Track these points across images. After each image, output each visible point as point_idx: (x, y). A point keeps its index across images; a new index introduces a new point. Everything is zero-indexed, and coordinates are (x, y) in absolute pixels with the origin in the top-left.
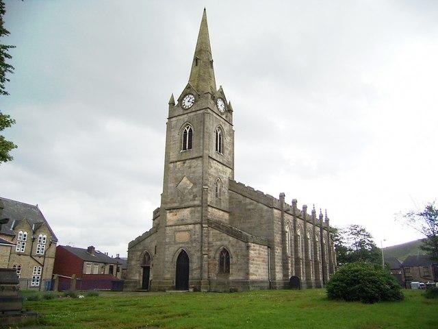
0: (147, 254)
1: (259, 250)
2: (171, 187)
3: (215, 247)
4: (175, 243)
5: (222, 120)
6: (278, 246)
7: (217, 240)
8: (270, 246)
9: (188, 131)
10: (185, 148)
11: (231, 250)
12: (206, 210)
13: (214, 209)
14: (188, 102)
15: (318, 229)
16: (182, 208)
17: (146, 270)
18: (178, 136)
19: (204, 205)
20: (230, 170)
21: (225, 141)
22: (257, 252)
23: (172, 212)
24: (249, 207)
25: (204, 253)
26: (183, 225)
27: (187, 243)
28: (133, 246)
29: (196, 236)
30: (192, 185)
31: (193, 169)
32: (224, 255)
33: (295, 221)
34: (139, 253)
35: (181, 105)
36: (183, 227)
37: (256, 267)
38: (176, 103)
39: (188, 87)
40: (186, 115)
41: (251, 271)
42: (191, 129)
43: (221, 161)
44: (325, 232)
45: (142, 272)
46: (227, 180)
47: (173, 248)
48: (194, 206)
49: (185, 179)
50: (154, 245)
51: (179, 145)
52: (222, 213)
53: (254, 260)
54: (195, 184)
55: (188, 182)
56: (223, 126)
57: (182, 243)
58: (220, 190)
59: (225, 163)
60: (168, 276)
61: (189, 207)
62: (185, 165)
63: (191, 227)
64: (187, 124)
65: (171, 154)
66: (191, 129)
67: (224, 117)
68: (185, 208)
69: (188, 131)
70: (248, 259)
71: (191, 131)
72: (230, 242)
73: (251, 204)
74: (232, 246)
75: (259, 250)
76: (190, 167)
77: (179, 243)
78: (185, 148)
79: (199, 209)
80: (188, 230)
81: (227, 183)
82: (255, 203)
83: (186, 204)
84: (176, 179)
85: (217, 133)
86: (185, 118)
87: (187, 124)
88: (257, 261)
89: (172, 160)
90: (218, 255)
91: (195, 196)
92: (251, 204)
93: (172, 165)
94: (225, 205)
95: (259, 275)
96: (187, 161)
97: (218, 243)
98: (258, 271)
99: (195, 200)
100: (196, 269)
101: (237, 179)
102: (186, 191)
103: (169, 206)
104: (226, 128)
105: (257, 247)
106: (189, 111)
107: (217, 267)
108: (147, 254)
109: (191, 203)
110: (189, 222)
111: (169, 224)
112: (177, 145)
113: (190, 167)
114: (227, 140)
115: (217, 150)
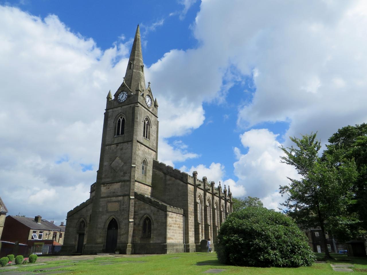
1: (175, 218)
2: (106, 166)
3: (141, 216)
4: (107, 212)
5: (149, 112)
6: (192, 215)
7: (141, 210)
8: (185, 215)
10: (118, 134)
11: (153, 217)
12: (134, 184)
15: (223, 201)
16: (114, 183)
17: (81, 235)
19: (132, 180)
20: (155, 153)
21: (151, 129)
22: (174, 219)
23: (106, 186)
24: (168, 182)
25: (131, 220)
26: (113, 196)
28: (71, 215)
29: (125, 206)
30: (123, 164)
32: (147, 222)
33: (205, 195)
34: (76, 221)
36: (114, 199)
37: (173, 232)
38: (113, 98)
39: (123, 85)
40: (120, 108)
42: (124, 118)
43: (148, 145)
44: (228, 204)
45: (77, 238)
46: (152, 160)
47: (105, 216)
48: (124, 181)
49: (118, 158)
50: (90, 212)
52: (146, 187)
53: (171, 226)
55: (120, 161)
56: (150, 117)
57: (112, 212)
58: (146, 168)
59: (150, 147)
60: (100, 240)
61: (119, 182)
62: (118, 147)
63: (120, 198)
65: (107, 138)
66: (124, 118)
67: (150, 110)
68: (117, 182)
70: (166, 226)
71: (123, 120)
72: (152, 211)
73: (170, 180)
74: (154, 214)
75: (175, 218)
76: (122, 149)
78: (118, 134)
80: (118, 201)
81: (152, 163)
82: (174, 179)
85: (145, 123)
88: (173, 227)
90: (142, 222)
92: (170, 180)
93: (107, 148)
94: (149, 181)
96: (119, 145)
97: (142, 212)
98: (174, 236)
101: (160, 160)
102: (118, 168)
103: (103, 181)
104: (152, 119)
105: (174, 215)
107: (141, 232)
108: (83, 222)
109: (123, 178)
110: (119, 194)
111: (102, 196)
113: (122, 149)
114: (153, 128)
115: (144, 136)
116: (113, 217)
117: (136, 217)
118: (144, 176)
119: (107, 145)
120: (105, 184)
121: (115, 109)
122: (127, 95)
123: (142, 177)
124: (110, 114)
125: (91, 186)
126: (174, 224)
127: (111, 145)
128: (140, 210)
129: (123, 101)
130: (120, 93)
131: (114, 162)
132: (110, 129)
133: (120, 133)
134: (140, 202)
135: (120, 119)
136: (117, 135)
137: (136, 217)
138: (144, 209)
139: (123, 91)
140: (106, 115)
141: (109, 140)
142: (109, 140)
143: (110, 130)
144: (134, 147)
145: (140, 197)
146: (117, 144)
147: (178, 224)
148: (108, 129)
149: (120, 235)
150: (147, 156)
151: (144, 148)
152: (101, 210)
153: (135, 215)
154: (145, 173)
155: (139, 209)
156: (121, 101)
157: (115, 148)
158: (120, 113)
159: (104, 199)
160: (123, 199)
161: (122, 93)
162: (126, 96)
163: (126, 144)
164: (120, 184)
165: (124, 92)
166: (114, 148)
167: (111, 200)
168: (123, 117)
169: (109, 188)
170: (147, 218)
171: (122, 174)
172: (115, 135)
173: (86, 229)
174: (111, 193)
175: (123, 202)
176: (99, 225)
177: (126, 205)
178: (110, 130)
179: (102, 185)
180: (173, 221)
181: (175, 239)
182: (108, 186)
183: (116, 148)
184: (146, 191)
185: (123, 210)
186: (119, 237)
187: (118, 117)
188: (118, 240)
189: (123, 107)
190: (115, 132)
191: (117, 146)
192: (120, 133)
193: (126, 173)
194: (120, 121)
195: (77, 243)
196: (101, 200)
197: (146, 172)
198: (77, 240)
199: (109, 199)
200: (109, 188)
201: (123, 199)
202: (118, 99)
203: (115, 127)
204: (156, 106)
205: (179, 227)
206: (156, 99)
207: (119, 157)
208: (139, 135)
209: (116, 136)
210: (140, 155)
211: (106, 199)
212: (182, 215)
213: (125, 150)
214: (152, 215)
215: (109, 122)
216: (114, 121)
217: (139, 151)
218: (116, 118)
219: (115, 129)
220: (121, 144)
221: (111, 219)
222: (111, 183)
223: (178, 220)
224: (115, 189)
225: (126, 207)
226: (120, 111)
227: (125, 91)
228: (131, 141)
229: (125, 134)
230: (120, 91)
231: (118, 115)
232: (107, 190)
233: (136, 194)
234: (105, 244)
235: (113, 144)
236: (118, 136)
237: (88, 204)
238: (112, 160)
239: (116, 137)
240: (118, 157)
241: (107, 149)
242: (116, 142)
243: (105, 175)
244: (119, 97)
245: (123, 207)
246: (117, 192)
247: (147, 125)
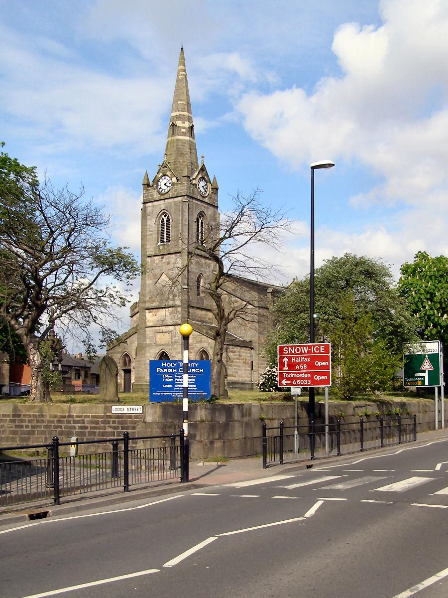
0: (127, 355)
1: (239, 352)
2: (149, 285)
3: (196, 349)
4: (157, 345)
9: (165, 221)
16: (162, 308)
18: (153, 224)
27: (168, 345)
29: (177, 338)
34: (119, 355)
35: (157, 187)
40: (162, 201)
41: (229, 372)
45: (123, 375)
49: (164, 276)
50: (135, 345)
51: (155, 236)
53: (232, 362)
57: (163, 345)
61: (169, 307)
62: (164, 260)
65: (148, 246)
67: (206, 200)
69: (165, 221)
71: (168, 220)
73: (236, 302)
75: (239, 352)
76: (168, 263)
77: (160, 345)
79: (179, 309)
80: (168, 332)
84: (155, 275)
85: (198, 221)
86: (161, 205)
87: (164, 213)
88: (236, 362)
89: (148, 253)
93: (149, 260)
95: (239, 376)
103: (148, 305)
105: (237, 349)
106: (166, 196)
111: (149, 324)
112: (153, 236)
113: (168, 263)
124: (149, 210)
126: (237, 359)
127: (154, 256)
128: (195, 342)
133: (165, 240)
135: (163, 219)
136: (161, 242)
138: (201, 342)
139: (164, 175)
140: (144, 211)
147: (242, 360)
148: (148, 233)
156: (163, 191)
159: (151, 328)
160: (175, 329)
166: (158, 260)
167: (159, 330)
172: (158, 242)
173: (133, 365)
174: (159, 321)
178: (152, 234)
179: (147, 311)
180: (235, 355)
181: (239, 376)
183: (162, 260)
185: (176, 342)
190: (158, 238)
191: (162, 258)
192: (165, 240)
194: (164, 221)
195: (123, 381)
196: (147, 329)
200: (156, 315)
201: (175, 329)
202: (159, 187)
203: (158, 231)
204: (215, 190)
205: (245, 363)
206: (215, 178)
209: (160, 243)
211: (153, 328)
214: (209, 349)
215: (149, 223)
216: (155, 222)
218: (159, 216)
219: (158, 233)
220: (168, 256)
222: (158, 308)
223: (241, 354)
230: (161, 174)
236: (162, 243)
247: (202, 223)
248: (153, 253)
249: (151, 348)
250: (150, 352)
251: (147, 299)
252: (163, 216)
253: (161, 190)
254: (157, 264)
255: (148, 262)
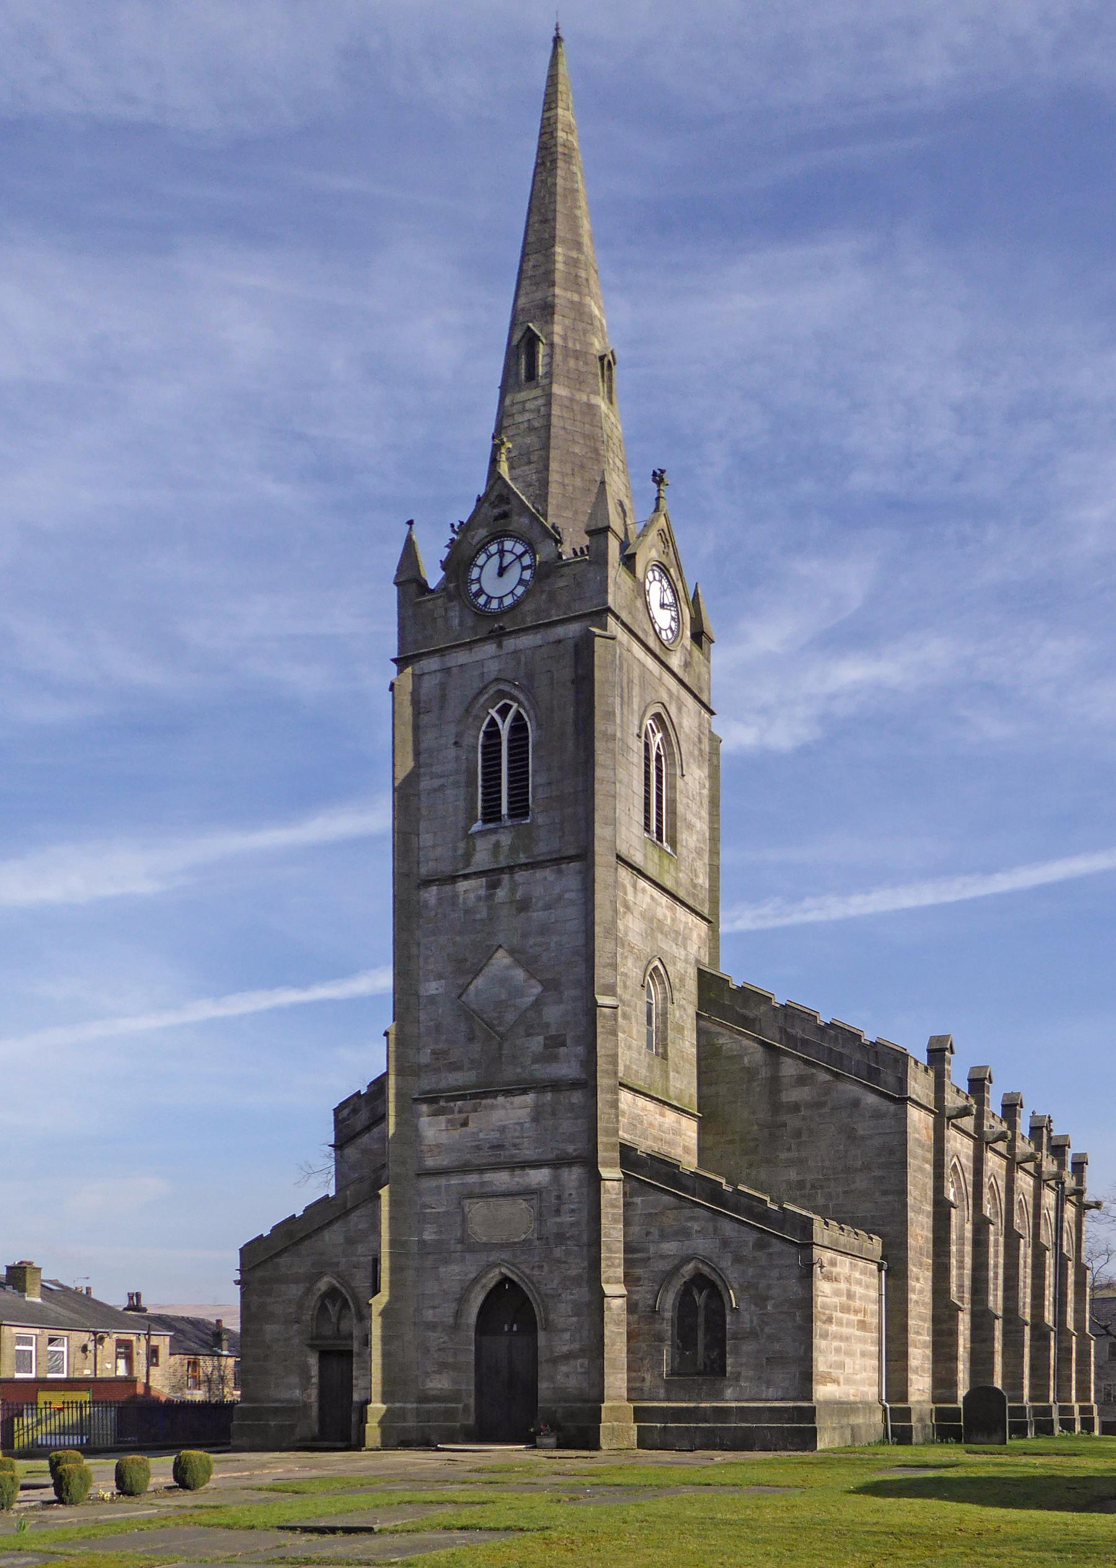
2: (432, 999)
4: (468, 1245)
7: (664, 1236)
9: (504, 729)
10: (491, 813)
12: (615, 1104)
13: (641, 1101)
14: (498, 582)
16: (494, 1094)
19: (603, 1081)
26: (496, 1167)
28: (260, 1261)
29: (568, 1219)
30: (537, 989)
31: (538, 916)
32: (700, 1299)
36: (501, 1179)
38: (434, 577)
40: (490, 648)
42: (518, 717)
45: (315, 1371)
47: (456, 1268)
48: (555, 1086)
49: (502, 959)
54: (551, 986)
55: (519, 974)
58: (664, 1014)
60: (439, 1383)
61: (524, 1091)
62: (501, 894)
63: (539, 1177)
64: (501, 694)
65: (426, 839)
69: (504, 729)
71: (519, 727)
76: (524, 905)
77: (488, 1247)
78: (491, 813)
80: (527, 1193)
83: (509, 1073)
87: (501, 694)
91: (555, 1042)
93: (431, 895)
99: (554, 1058)
100: (567, 1357)
102: (510, 1017)
108: (332, 1293)
111: (430, 1162)
116: (504, 1270)
117: (639, 1271)
118: (657, 1061)
119: (427, 883)
120: (442, 1103)
121: (461, 657)
122: (527, 560)
123: (650, 1068)
125: (337, 1111)
127: (453, 879)
129: (508, 601)
130: (483, 547)
131: (479, 982)
132: (436, 783)
133: (504, 810)
134: (653, 1197)
135: (493, 723)
137: (639, 1271)
139: (498, 536)
141: (435, 851)
142: (435, 851)
143: (435, 790)
144: (601, 897)
145: (647, 1169)
146: (492, 876)
149: (554, 1361)
150: (668, 946)
151: (652, 897)
152: (433, 1237)
153: (628, 1263)
154: (659, 1045)
155: (648, 1234)
156: (494, 604)
157: (479, 898)
158: (497, 680)
159: (442, 1181)
160: (556, 1179)
161: (493, 548)
162: (524, 568)
163: (548, 874)
164: (530, 1098)
165: (508, 545)
168: (515, 705)
169: (465, 1124)
170: (699, 1281)
171: (536, 1044)
175: (559, 1197)
176: (431, 1312)
177: (573, 1211)
178: (442, 788)
179: (424, 1108)
182: (460, 1112)
184: (678, 1137)
186: (544, 1370)
187: (485, 709)
188: (543, 1386)
189: (511, 643)
191: (493, 886)
192: (504, 810)
193: (564, 1044)
194: (497, 734)
195: (314, 1393)
197: (663, 1041)
198: (315, 1380)
199: (473, 1178)
202: (474, 588)
207: (511, 952)
208: (621, 825)
209: (477, 826)
210: (634, 939)
211: (455, 1181)
212: (874, 1267)
213: (548, 907)
217: (629, 917)
221: (492, 1279)
222: (475, 1096)
224: (502, 1129)
225: (572, 1224)
226: (493, 668)
227: (518, 538)
228: (585, 856)
229: (538, 816)
230: (482, 532)
231: (481, 693)
232: (457, 1133)
233: (628, 1156)
234: (472, 1401)
235: (466, 877)
236: (491, 826)
237: (355, 1207)
238: (468, 967)
239: (481, 833)
240: (501, 953)
241: (433, 901)
242: (482, 858)
243: (433, 1052)
244: (475, 573)
245: (558, 1220)
246: (515, 1145)
248: (446, 868)
249: (446, 1262)
250: (438, 1279)
251: (425, 1057)
252: (493, 712)
253: (482, 600)
254: (467, 912)
255: (426, 905)
